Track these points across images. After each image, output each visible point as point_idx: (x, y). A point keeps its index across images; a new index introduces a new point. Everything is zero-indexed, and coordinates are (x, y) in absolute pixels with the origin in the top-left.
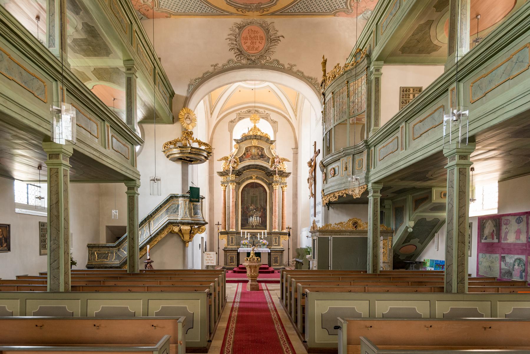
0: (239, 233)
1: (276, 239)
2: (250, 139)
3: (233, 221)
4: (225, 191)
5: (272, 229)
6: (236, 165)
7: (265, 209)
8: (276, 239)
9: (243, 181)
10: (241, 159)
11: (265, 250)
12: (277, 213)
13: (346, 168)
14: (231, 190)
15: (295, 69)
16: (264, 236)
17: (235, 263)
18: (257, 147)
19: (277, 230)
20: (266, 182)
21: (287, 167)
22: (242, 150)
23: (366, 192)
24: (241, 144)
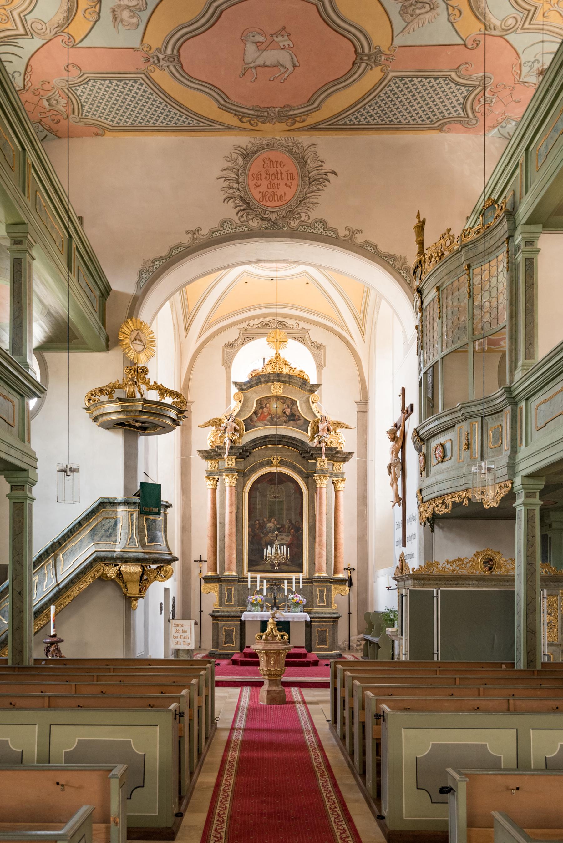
0: (244, 580)
1: (322, 592)
2: (267, 382)
3: (231, 554)
4: (214, 491)
5: (314, 571)
6: (237, 435)
7: (299, 529)
8: (322, 592)
9: (253, 470)
10: (249, 424)
11: (298, 616)
12: (324, 538)
13: (468, 445)
14: (228, 489)
15: (360, 239)
16: (297, 587)
17: (236, 644)
18: (282, 398)
19: (324, 574)
20: (300, 473)
21: (345, 441)
22: (250, 404)
23: (511, 496)
24: (249, 393)
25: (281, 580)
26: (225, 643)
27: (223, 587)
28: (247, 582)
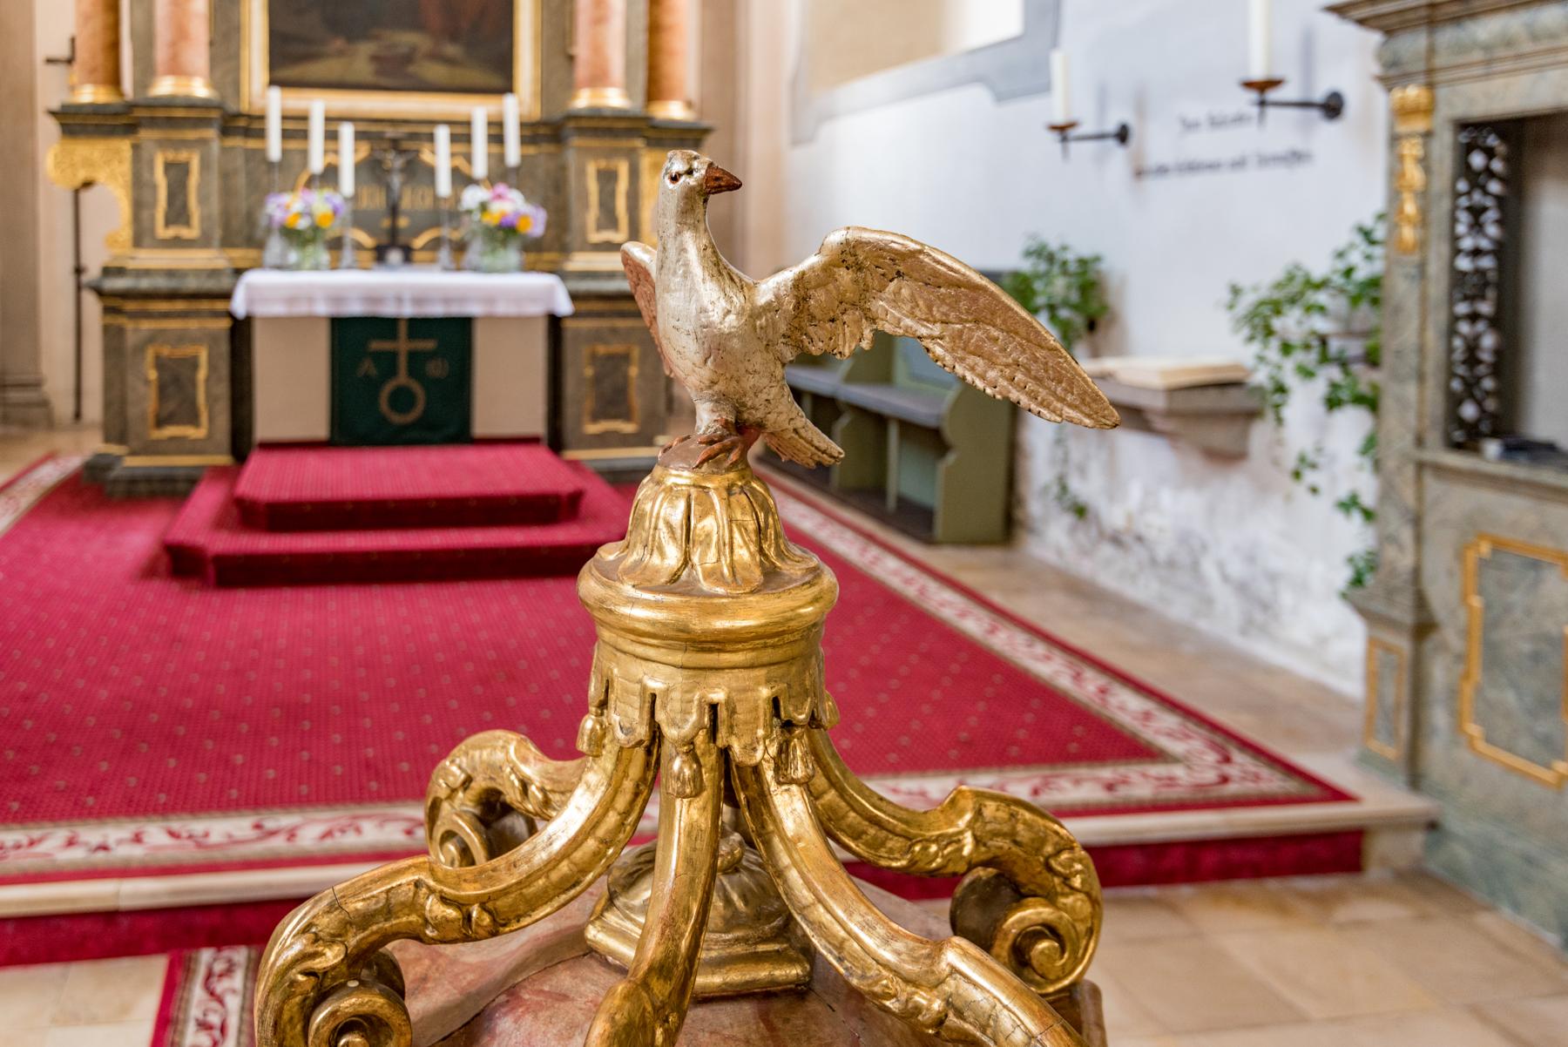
0: (240, 124)
1: (607, 178)
5: (570, 87)
8: (607, 178)
11: (506, 292)
16: (498, 159)
17: (207, 428)
19: (614, 99)
25: (421, 131)
26: (161, 422)
27: (145, 154)
28: (261, 134)
